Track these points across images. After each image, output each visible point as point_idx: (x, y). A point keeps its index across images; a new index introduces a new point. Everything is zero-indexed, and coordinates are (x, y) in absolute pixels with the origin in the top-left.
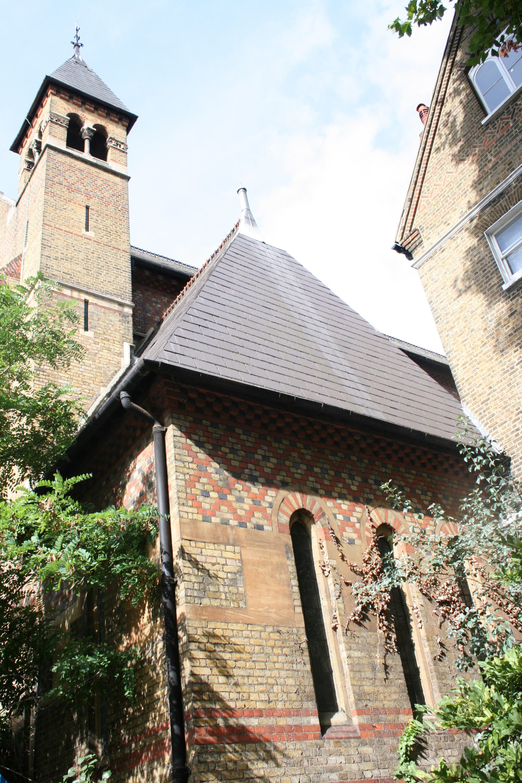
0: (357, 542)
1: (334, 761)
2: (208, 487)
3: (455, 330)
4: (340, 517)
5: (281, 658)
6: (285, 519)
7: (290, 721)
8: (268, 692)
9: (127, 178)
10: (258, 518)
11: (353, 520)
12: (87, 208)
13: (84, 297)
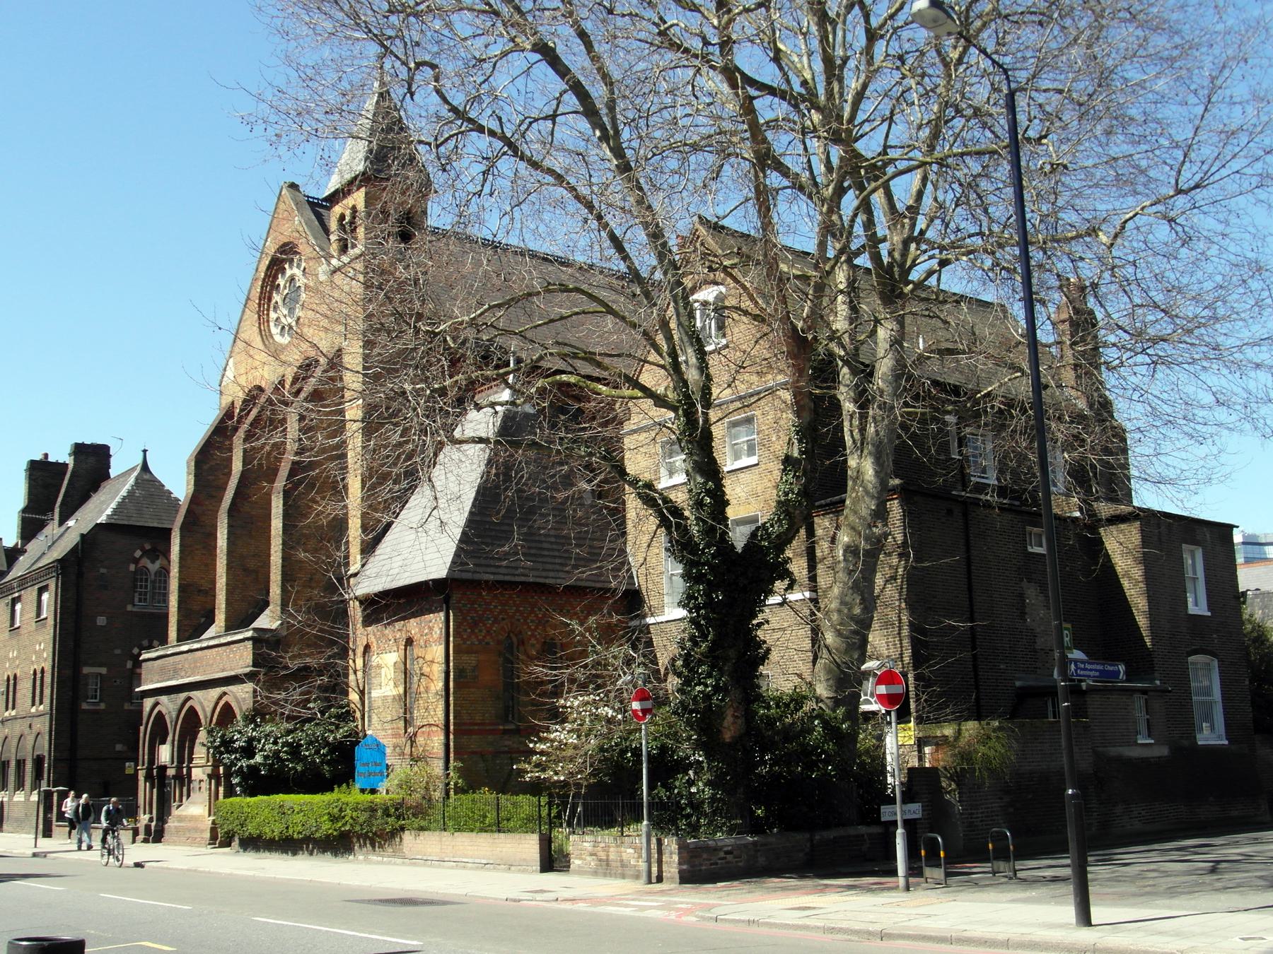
1: (507, 743)
7: (491, 727)
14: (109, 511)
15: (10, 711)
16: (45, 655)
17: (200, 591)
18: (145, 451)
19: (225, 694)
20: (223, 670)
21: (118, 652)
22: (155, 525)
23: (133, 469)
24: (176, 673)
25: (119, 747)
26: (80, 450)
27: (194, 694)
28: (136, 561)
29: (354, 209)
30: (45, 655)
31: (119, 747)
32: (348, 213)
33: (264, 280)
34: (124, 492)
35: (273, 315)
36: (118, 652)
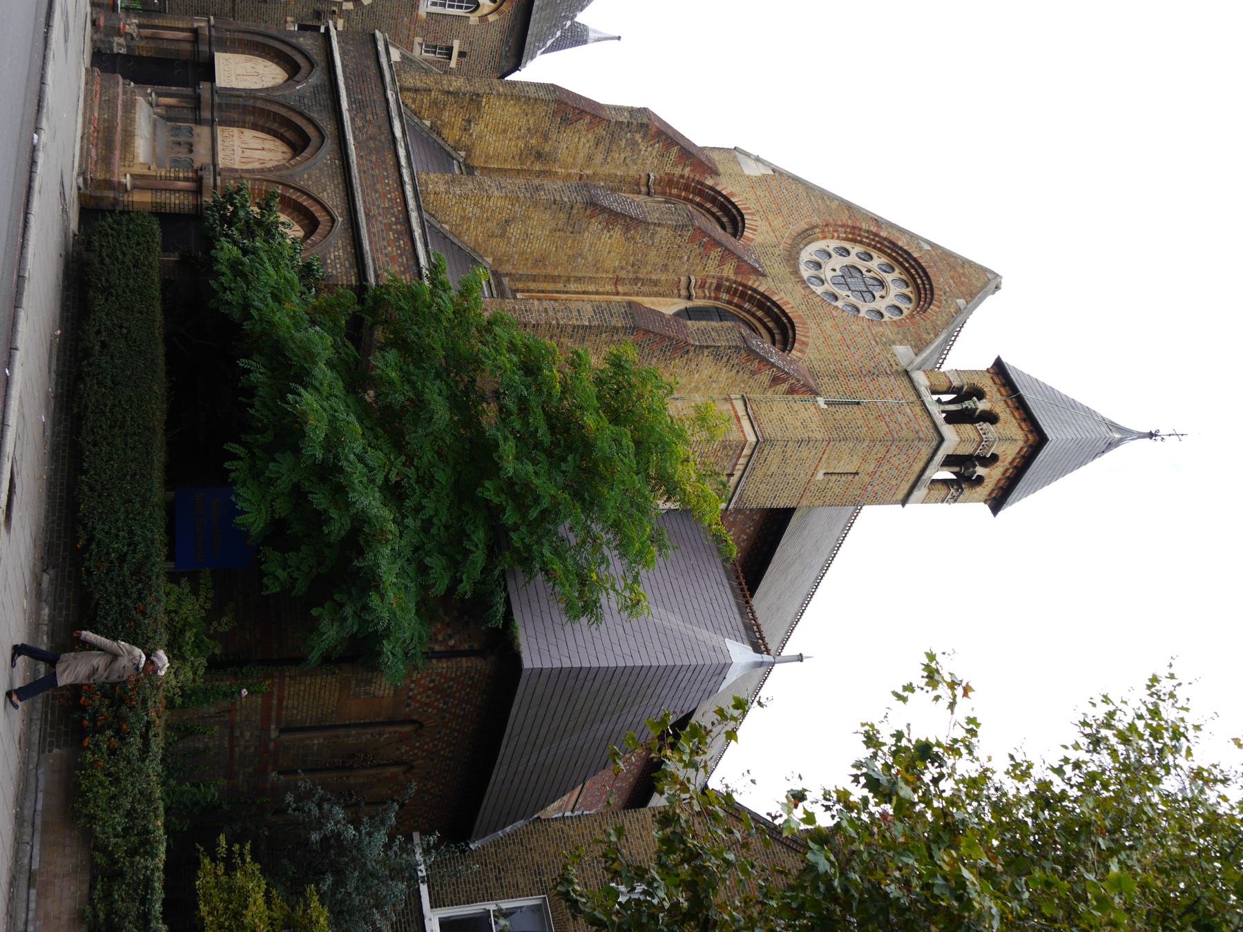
0: (398, 753)
1: (247, 735)
2: (437, 683)
3: (598, 829)
4: (418, 744)
5: (314, 714)
6: (415, 717)
8: (293, 708)
10: (414, 705)
11: (416, 751)
12: (857, 473)
13: (737, 474)
17: (469, 121)
19: (333, 220)
20: (367, 215)
24: (358, 106)
27: (329, 144)
29: (991, 418)
32: (982, 405)
33: (876, 235)
35: (832, 244)
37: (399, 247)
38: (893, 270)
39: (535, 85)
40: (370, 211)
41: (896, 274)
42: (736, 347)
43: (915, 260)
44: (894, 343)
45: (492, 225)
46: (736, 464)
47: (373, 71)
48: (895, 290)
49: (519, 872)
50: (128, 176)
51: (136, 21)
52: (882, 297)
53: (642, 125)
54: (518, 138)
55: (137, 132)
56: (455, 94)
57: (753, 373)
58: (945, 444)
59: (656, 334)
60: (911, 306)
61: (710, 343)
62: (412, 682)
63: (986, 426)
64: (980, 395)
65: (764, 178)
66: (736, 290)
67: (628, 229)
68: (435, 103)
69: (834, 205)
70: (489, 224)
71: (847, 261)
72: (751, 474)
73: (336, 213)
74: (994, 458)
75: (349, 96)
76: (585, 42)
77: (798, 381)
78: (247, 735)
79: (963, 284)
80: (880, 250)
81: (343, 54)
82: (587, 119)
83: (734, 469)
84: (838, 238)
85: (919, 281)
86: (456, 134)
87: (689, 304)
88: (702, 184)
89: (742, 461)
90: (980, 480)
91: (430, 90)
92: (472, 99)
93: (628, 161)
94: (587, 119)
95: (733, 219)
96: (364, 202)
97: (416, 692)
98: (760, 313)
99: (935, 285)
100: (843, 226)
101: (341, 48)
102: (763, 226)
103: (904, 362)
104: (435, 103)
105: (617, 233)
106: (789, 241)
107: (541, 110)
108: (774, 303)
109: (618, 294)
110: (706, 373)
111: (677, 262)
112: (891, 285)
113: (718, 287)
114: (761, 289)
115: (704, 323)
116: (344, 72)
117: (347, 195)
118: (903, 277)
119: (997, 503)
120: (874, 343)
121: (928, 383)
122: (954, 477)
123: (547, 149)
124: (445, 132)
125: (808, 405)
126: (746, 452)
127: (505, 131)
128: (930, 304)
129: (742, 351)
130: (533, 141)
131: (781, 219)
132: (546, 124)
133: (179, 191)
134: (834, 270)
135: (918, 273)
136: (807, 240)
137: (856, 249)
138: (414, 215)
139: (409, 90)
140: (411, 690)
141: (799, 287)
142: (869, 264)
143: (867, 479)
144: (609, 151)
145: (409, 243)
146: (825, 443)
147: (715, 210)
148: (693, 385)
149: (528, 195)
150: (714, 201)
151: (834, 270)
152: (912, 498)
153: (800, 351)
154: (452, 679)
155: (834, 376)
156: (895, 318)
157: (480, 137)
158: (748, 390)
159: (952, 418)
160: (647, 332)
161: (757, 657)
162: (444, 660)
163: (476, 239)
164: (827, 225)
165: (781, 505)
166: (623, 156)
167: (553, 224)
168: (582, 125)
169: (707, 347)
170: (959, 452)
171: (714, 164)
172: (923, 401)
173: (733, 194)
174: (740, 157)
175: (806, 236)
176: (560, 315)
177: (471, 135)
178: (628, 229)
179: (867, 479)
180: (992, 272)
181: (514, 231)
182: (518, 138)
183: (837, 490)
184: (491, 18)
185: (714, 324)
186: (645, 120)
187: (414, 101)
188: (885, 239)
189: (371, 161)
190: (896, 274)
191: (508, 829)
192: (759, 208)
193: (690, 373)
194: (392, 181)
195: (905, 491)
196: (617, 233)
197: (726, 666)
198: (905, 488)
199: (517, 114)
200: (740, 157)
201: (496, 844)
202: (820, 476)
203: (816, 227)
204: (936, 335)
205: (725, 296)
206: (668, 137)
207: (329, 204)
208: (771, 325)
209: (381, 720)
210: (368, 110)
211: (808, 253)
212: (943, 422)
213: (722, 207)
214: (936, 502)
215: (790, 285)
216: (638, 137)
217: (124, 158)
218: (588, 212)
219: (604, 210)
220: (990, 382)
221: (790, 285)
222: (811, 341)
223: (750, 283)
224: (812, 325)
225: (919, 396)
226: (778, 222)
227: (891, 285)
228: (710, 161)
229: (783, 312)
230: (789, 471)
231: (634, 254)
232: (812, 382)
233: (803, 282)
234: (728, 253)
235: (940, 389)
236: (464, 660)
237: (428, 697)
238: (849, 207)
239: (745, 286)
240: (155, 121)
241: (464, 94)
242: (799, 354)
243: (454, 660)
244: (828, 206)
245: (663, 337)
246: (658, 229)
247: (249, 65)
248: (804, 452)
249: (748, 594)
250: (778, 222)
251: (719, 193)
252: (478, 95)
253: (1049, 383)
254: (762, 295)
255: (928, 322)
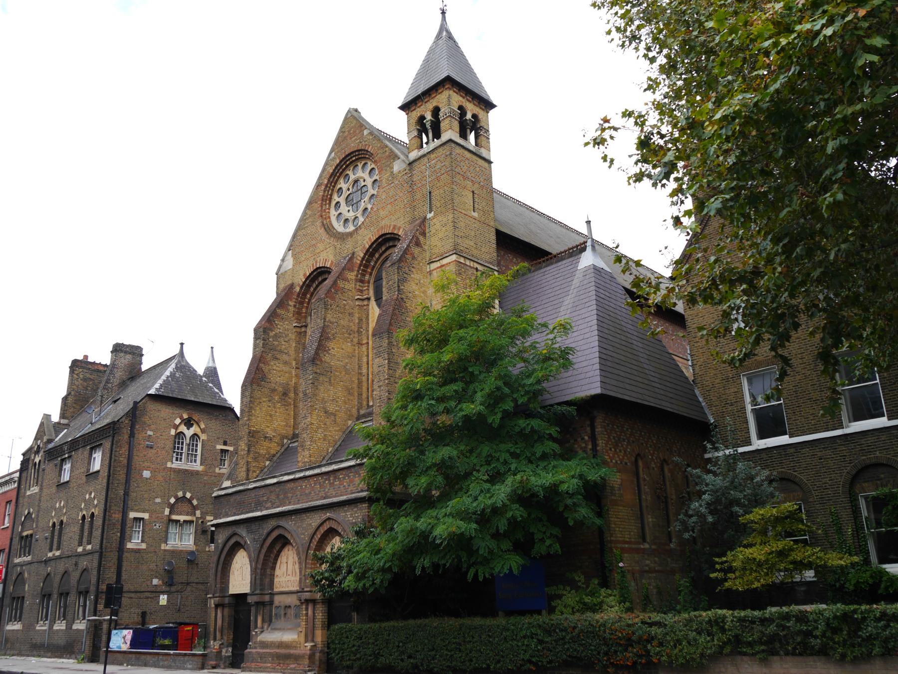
1: (648, 562)
3: (699, 344)
6: (633, 459)
9: (490, 162)
10: (626, 460)
12: (473, 192)
13: (476, 265)
14: (157, 386)
15: (54, 552)
16: (96, 502)
18: (182, 344)
19: (329, 519)
20: (325, 498)
21: (158, 500)
22: (192, 399)
23: (174, 357)
24: (259, 506)
25: (155, 581)
26: (118, 349)
27: (282, 522)
28: (176, 427)
29: (436, 111)
30: (96, 502)
31: (155, 581)
32: (429, 117)
33: (326, 186)
34: (167, 373)
35: (333, 213)
36: (158, 500)
37: (344, 478)
38: (347, 175)
39: (242, 398)
40: (322, 496)
41: (350, 173)
42: (398, 269)
43: (341, 162)
44: (392, 172)
45: (328, 422)
46: (470, 266)
47: (238, 497)
48: (360, 173)
49: (727, 391)
50: (306, 644)
51: (212, 642)
52: (364, 181)
53: (264, 332)
54: (275, 407)
55: (279, 640)
56: (249, 446)
57: (414, 258)
58: (453, 138)
59: (392, 319)
60: (369, 163)
61: (396, 285)
62: (612, 462)
63: (441, 114)
64: (422, 118)
65: (294, 256)
66: (363, 270)
67: (328, 338)
68: (255, 459)
69: (309, 212)
70: (328, 423)
71: (343, 203)
72: (476, 257)
73: (324, 517)
74: (461, 108)
75: (253, 511)
76: (215, 368)
77: (417, 230)
78: (648, 562)
79: (354, 132)
80: (336, 183)
81: (227, 516)
82: (262, 365)
83: (473, 268)
84: (329, 209)
85: (354, 158)
86: (273, 445)
87: (373, 299)
88: (299, 294)
89: (468, 263)
90: (474, 116)
91: (248, 462)
92: (252, 436)
93: (286, 340)
94: (262, 365)
95: (319, 274)
96: (317, 500)
97: (617, 459)
98: (377, 255)
99: (356, 149)
100: (322, 207)
101: (224, 517)
102: (323, 255)
103: (404, 166)
104: (255, 459)
105: (331, 345)
106: (332, 239)
107: (257, 394)
108: (370, 247)
109: (368, 343)
110: (414, 287)
111: (347, 307)
112: (357, 175)
113: (362, 281)
114: (362, 255)
115: (384, 289)
116: (238, 515)
117: (313, 511)
118: (351, 168)
119: (489, 105)
120: (393, 185)
121: (416, 150)
122: (473, 132)
123: (281, 389)
124: (273, 452)
125: (432, 223)
126: (462, 260)
127: (271, 416)
128: (367, 151)
129: (401, 265)
130: (276, 398)
131: (319, 245)
132: (266, 391)
133: (314, 613)
134: (349, 211)
135: (349, 159)
136: (331, 228)
137: (336, 198)
138: (324, 469)
139: (248, 475)
140: (616, 462)
141: (360, 232)
142: (344, 189)
143: (477, 186)
144: (281, 352)
145: (341, 472)
146: (455, 212)
147: (314, 285)
148: (422, 295)
149: (309, 400)
150: (309, 286)
151: (349, 211)
152: (487, 157)
153: (399, 230)
154: (609, 437)
155: (414, 208)
156: (377, 172)
157: (275, 430)
158: (424, 261)
159: (437, 135)
160: (390, 324)
161: (589, 249)
162: (597, 442)
163: (337, 431)
164: (322, 216)
165: (494, 237)
166: (283, 343)
167: (326, 384)
168: (265, 368)
169: (399, 287)
170: (458, 129)
171: (286, 287)
172: (427, 153)
173: (305, 275)
174: (282, 271)
175: (328, 229)
176: (382, 378)
177: (274, 436)
178: (328, 338)
179: (477, 186)
180: (347, 114)
181: (331, 408)
182: (275, 407)
183: (484, 204)
184: (203, 426)
185: (384, 283)
186: (261, 330)
187: (254, 471)
188: (329, 180)
189: (292, 497)
190: (350, 173)
191: (701, 399)
192: (313, 258)
193: (415, 297)
194: (304, 484)
195: (483, 162)
196: (331, 345)
197: (595, 268)
198: (481, 162)
199: (260, 409)
200: (282, 271)
201: (710, 406)
202: (475, 215)
203: (323, 223)
204: (387, 146)
205: (367, 277)
206: (271, 315)
207: (319, 521)
208: (383, 248)
209: (635, 480)
210: (261, 499)
211: (339, 227)
212: (440, 140)
213: (313, 281)
214: (489, 142)
215: (359, 238)
216: (272, 334)
217: (295, 647)
218: (318, 363)
219: (317, 353)
220: (414, 112)
221: (359, 238)
222: (393, 224)
223: (359, 262)
224: (383, 223)
225: (424, 156)
226: (321, 246)
227: (357, 175)
228: (284, 289)
229: (375, 241)
230: (473, 234)
231: (343, 334)
232: (418, 222)
233: (356, 229)
234: (341, 276)
235: (419, 143)
236: (597, 430)
237: (620, 451)
238: (310, 203)
239: (360, 265)
240: (272, 629)
241: (249, 441)
242: (401, 230)
243: (597, 436)
244: (310, 216)
245: (393, 314)
246: (327, 320)
247: (236, 573)
248: (461, 225)
249: (550, 256)
250: (321, 246)
251: (304, 283)
252: (249, 433)
253: (414, 76)
254: (365, 254)
255: (379, 152)
